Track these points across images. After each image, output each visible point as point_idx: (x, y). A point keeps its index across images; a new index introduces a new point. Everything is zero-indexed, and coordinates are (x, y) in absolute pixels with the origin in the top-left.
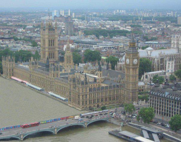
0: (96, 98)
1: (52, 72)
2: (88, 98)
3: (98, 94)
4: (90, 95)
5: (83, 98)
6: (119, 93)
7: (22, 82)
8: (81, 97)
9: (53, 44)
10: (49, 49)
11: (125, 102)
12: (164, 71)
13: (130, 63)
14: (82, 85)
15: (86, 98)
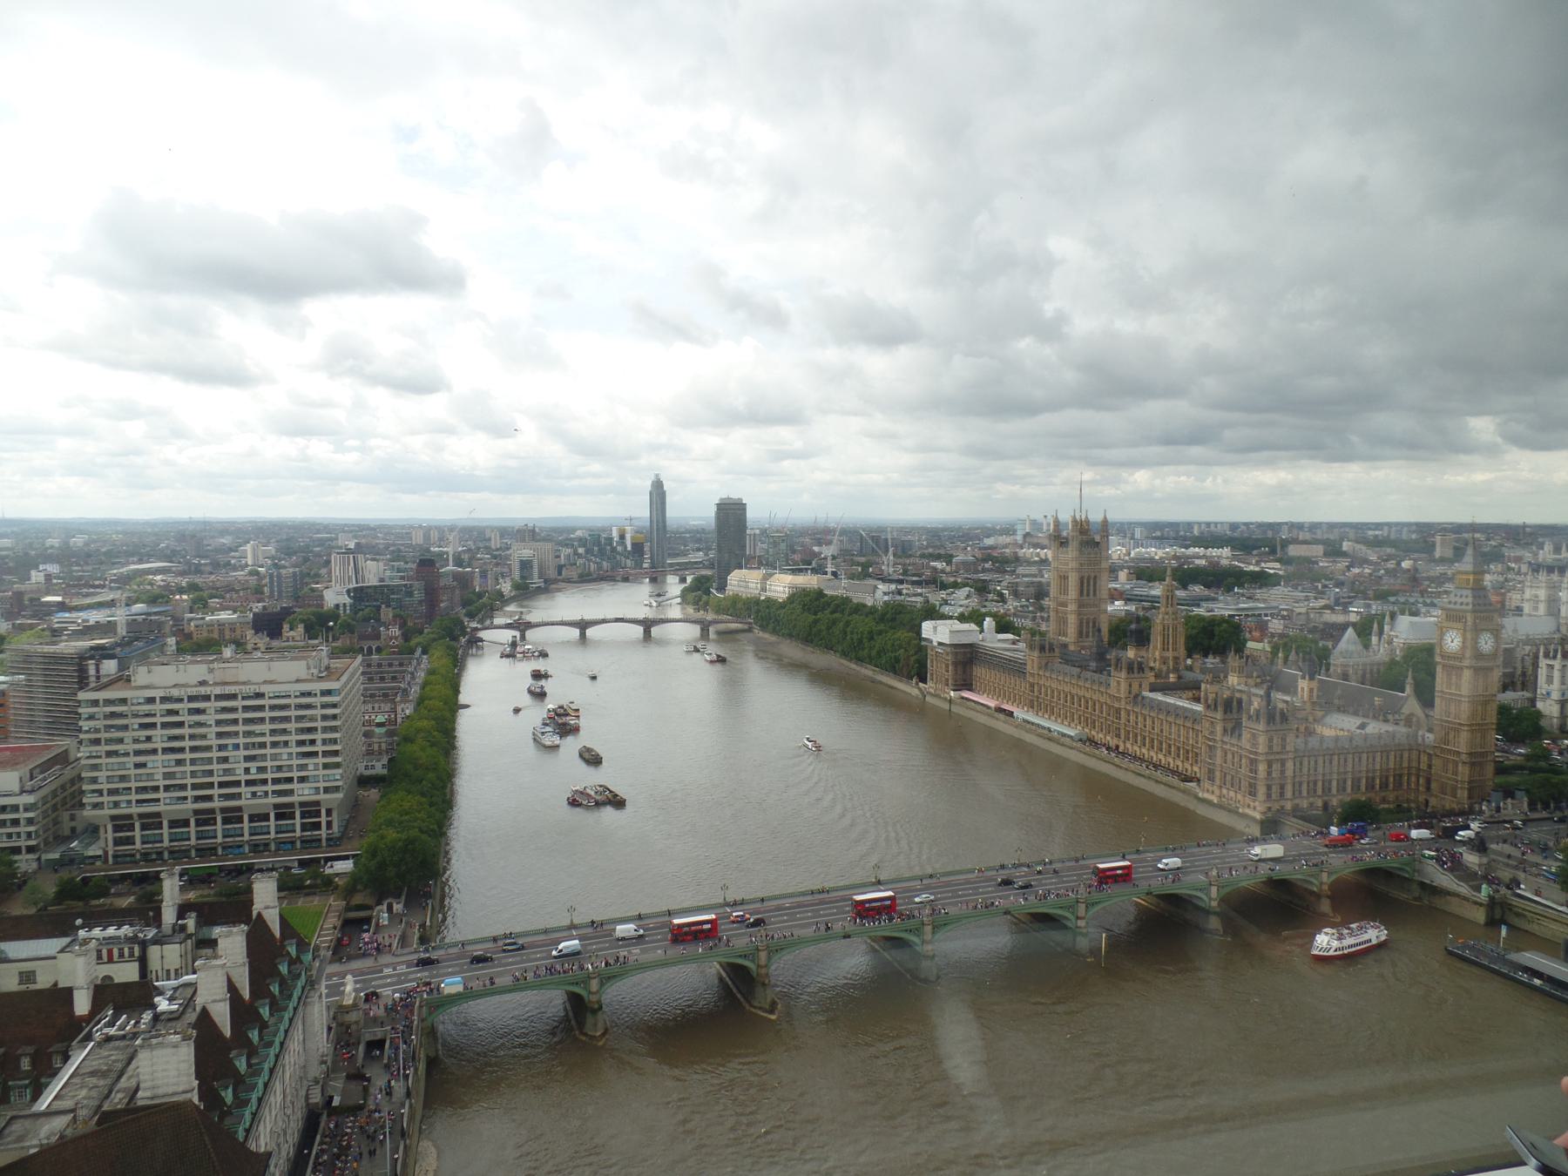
0: (1320, 778)
1: (1123, 674)
2: (1289, 773)
3: (1327, 761)
4: (1298, 764)
5: (1269, 773)
6: (1405, 764)
7: (999, 710)
8: (1262, 768)
9: (1095, 591)
10: (1079, 607)
11: (1433, 801)
12: (1527, 695)
13: (1464, 647)
14: (1268, 723)
15: (1283, 772)
